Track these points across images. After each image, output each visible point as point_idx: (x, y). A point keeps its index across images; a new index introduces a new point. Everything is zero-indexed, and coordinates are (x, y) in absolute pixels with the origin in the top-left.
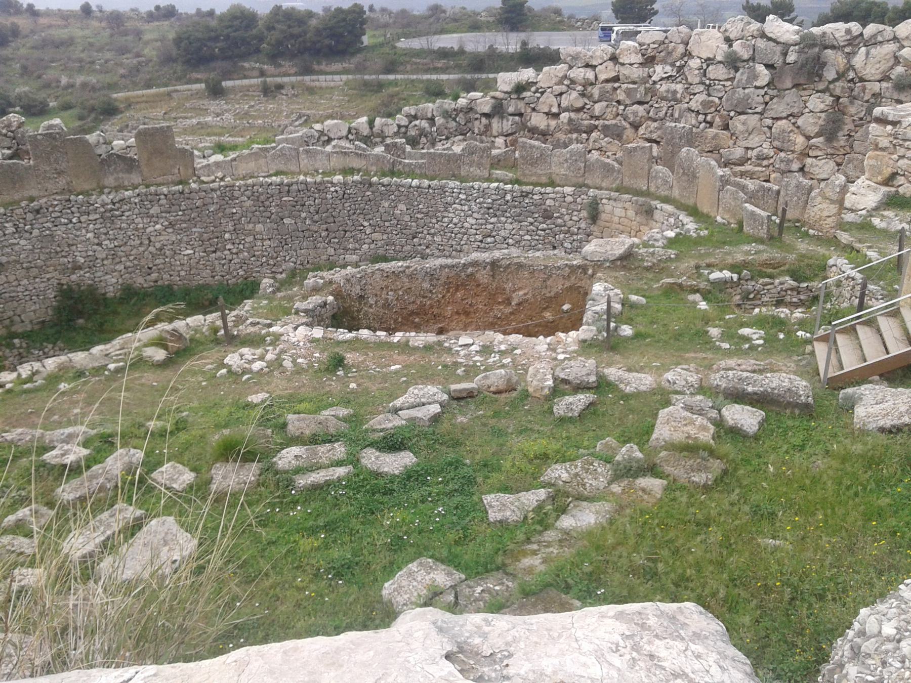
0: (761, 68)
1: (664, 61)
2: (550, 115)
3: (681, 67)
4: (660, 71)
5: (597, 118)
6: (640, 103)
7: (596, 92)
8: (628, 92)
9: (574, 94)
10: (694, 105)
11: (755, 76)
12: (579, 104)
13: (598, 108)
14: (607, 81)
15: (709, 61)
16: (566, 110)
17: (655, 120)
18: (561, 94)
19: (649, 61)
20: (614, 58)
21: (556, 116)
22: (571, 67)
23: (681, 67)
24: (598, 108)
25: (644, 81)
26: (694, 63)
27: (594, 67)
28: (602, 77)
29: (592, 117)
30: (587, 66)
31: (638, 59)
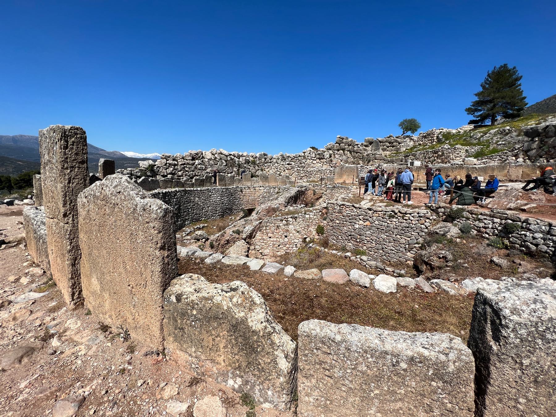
0: (224, 161)
1: (197, 159)
2: (164, 176)
3: (202, 161)
4: (197, 162)
5: (180, 176)
6: (193, 171)
7: (179, 168)
8: (189, 168)
9: (172, 169)
10: (208, 170)
11: (223, 163)
12: (173, 172)
13: (180, 173)
14: (181, 165)
15: (210, 159)
16: (170, 174)
17: (197, 176)
18: (166, 169)
19: (193, 159)
20: (182, 158)
21: (166, 176)
22: (167, 160)
23: (202, 161)
24: (180, 173)
25: (193, 164)
26: (206, 160)
27: (177, 161)
28: (180, 163)
29: (178, 176)
30: (174, 160)
31: (191, 158)
